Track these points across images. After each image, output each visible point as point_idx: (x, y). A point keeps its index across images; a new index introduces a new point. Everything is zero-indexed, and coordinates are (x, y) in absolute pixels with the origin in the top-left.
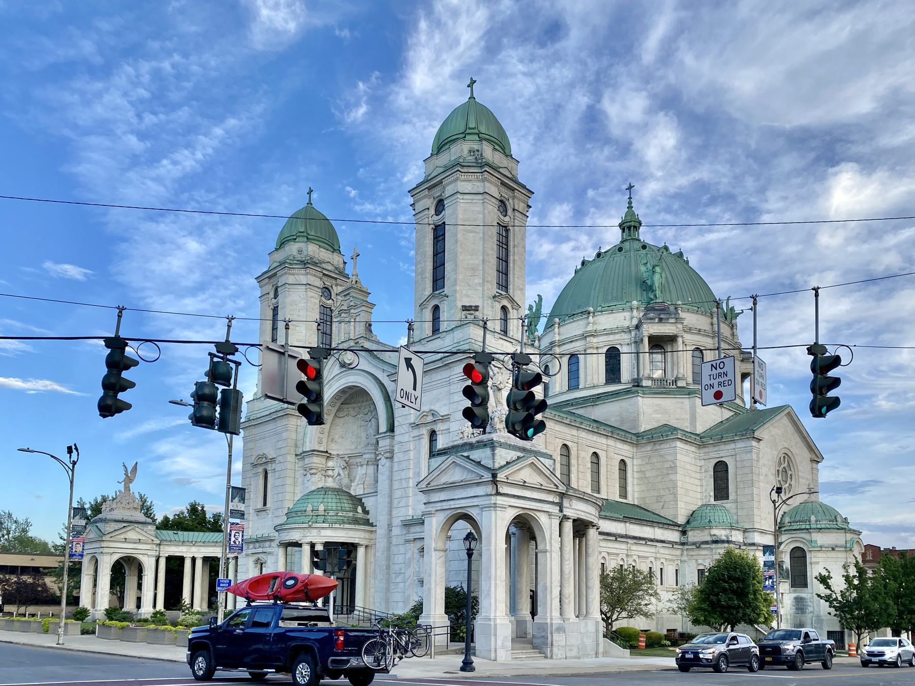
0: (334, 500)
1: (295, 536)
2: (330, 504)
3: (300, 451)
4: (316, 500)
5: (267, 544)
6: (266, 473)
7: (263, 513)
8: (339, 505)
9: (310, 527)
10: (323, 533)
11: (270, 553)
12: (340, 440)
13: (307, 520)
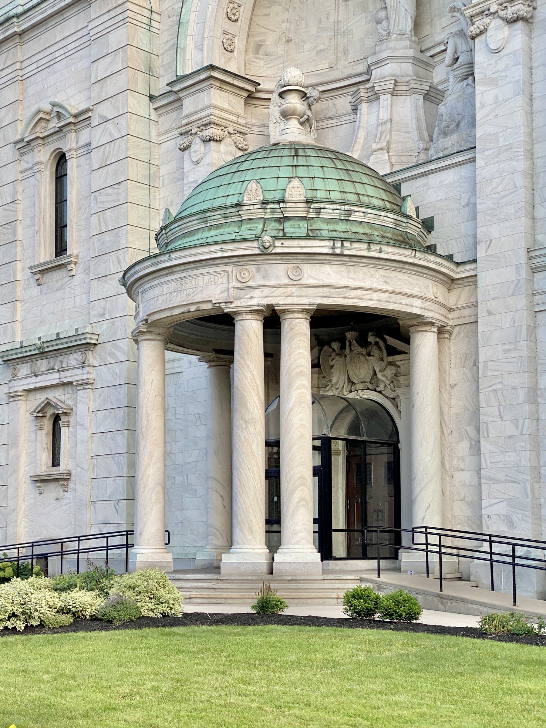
0: (332, 173)
1: (209, 290)
2: (319, 184)
3: (160, 86)
4: (274, 173)
5: (73, 359)
6: (61, 159)
7: (57, 275)
8: (349, 187)
9: (265, 253)
10: (312, 273)
11: (85, 384)
12: (281, 50)
13: (245, 231)
